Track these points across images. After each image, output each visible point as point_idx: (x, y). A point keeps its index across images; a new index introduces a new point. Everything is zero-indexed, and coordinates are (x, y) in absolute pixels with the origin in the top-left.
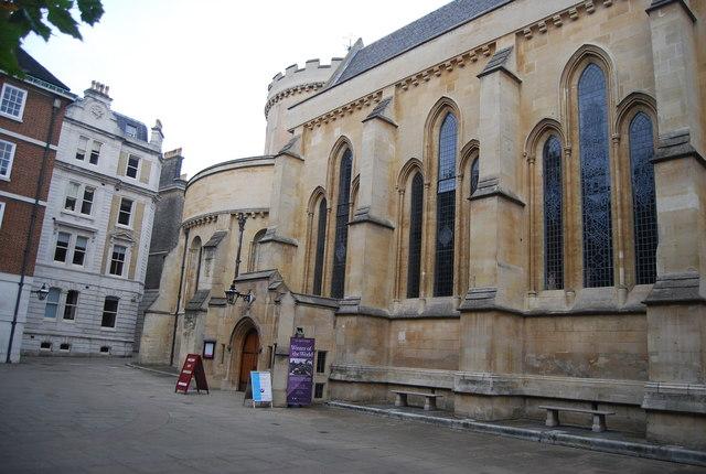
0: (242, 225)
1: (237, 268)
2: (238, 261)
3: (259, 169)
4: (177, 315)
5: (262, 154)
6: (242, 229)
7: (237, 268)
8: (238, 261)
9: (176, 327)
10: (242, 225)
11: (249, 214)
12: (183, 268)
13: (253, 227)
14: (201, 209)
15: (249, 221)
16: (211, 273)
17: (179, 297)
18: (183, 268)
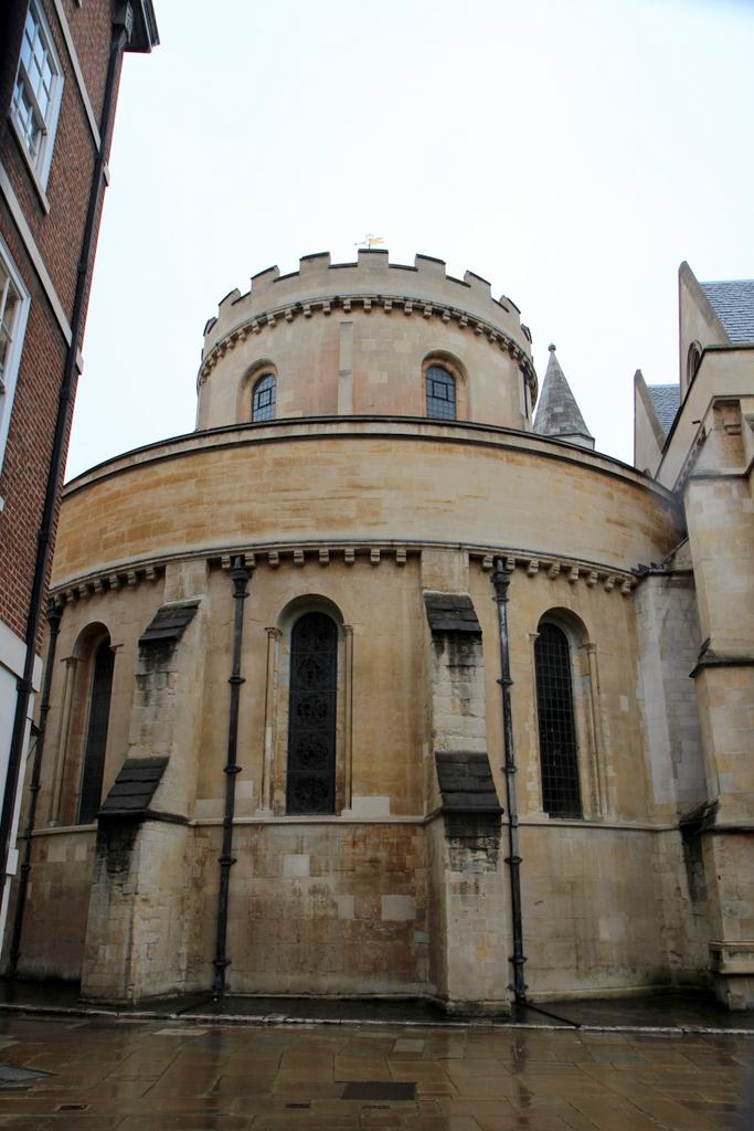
0: (501, 587)
1: (506, 699)
2: (505, 683)
3: (526, 459)
4: (228, 826)
5: (190, 428)
6: (501, 598)
7: (506, 699)
8: (505, 683)
9: (227, 862)
10: (501, 587)
11: (522, 565)
12: (236, 682)
13: (531, 600)
14: (331, 522)
15: (517, 581)
16: (478, 706)
17: (232, 771)
18: (236, 682)
